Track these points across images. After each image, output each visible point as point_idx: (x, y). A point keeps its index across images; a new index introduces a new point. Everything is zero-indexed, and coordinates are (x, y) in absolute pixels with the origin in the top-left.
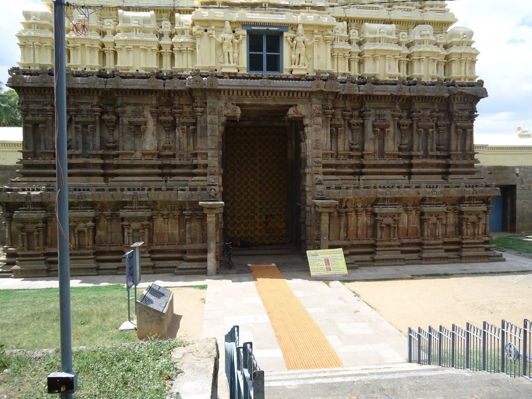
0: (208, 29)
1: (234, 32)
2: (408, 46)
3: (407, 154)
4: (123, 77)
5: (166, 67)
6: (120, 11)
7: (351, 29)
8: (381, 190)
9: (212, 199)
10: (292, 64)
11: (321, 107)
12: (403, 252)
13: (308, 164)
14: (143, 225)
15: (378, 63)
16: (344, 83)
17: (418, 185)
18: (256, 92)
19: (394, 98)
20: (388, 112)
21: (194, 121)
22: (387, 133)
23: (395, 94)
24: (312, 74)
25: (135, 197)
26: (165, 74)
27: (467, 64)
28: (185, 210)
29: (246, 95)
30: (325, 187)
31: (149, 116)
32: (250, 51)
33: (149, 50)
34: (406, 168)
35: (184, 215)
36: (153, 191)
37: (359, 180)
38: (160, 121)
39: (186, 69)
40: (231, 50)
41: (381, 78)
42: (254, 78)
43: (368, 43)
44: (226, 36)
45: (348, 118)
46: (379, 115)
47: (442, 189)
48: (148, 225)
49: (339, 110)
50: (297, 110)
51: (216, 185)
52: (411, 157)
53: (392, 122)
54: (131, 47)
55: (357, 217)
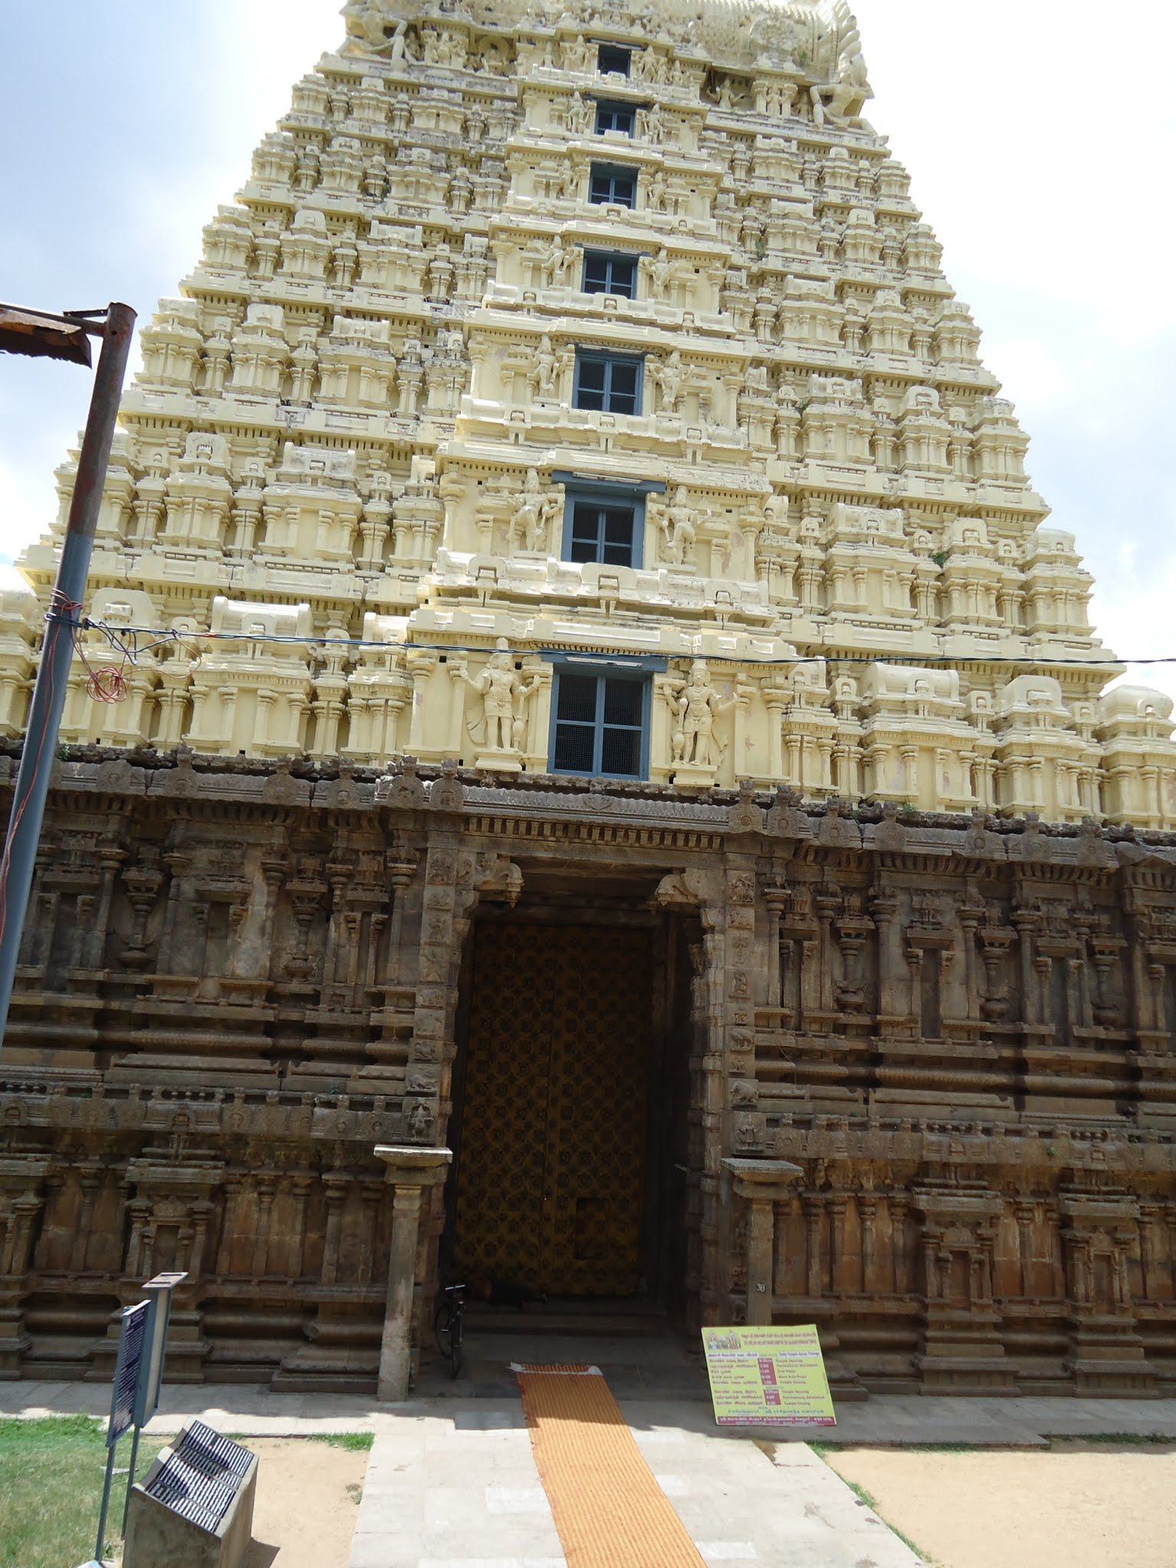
0: (448, 654)
1: (518, 666)
2: (996, 726)
3: (1007, 1028)
4: (199, 769)
5: (324, 747)
6: (219, 600)
7: (838, 676)
8: (933, 1137)
9: (414, 1139)
10: (673, 758)
11: (754, 879)
12: (1012, 1349)
13: (712, 1045)
14: (191, 1212)
15: (913, 768)
16: (820, 815)
17: (1047, 1128)
18: (570, 829)
19: (963, 866)
20: (946, 903)
21: (386, 900)
22: (944, 963)
23: (964, 853)
24: (728, 787)
25: (181, 1118)
26: (318, 766)
27: (1163, 785)
28: (330, 1169)
29: (541, 833)
30: (763, 1117)
31: (258, 878)
32: (559, 718)
33: (283, 701)
34: (1005, 1071)
35: (326, 1186)
36: (238, 1102)
37: (866, 1101)
38: (288, 894)
39: (377, 756)
40: (507, 712)
41: (924, 807)
42: (565, 790)
43: (883, 713)
44: (496, 674)
45: (831, 913)
46: (921, 911)
47: (1120, 1144)
48: (208, 1212)
49: (804, 889)
50: (683, 883)
51: (433, 1095)
52: (1019, 1040)
53: (958, 933)
54: (235, 690)
55: (863, 1221)
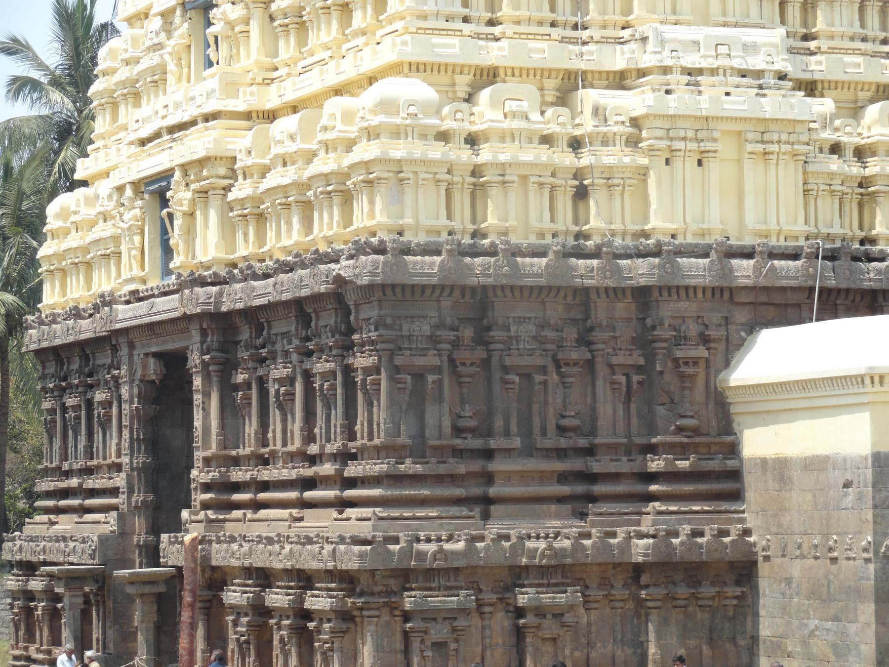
3: (475, 443)
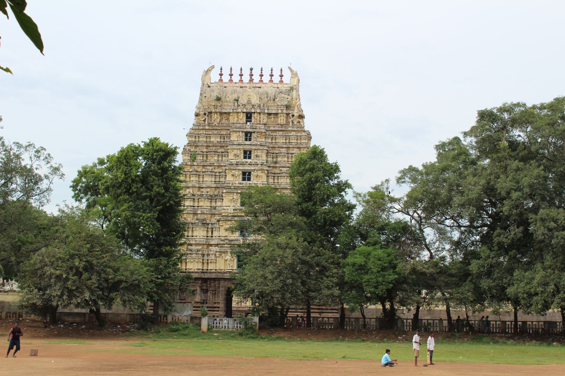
44: (228, 257)
